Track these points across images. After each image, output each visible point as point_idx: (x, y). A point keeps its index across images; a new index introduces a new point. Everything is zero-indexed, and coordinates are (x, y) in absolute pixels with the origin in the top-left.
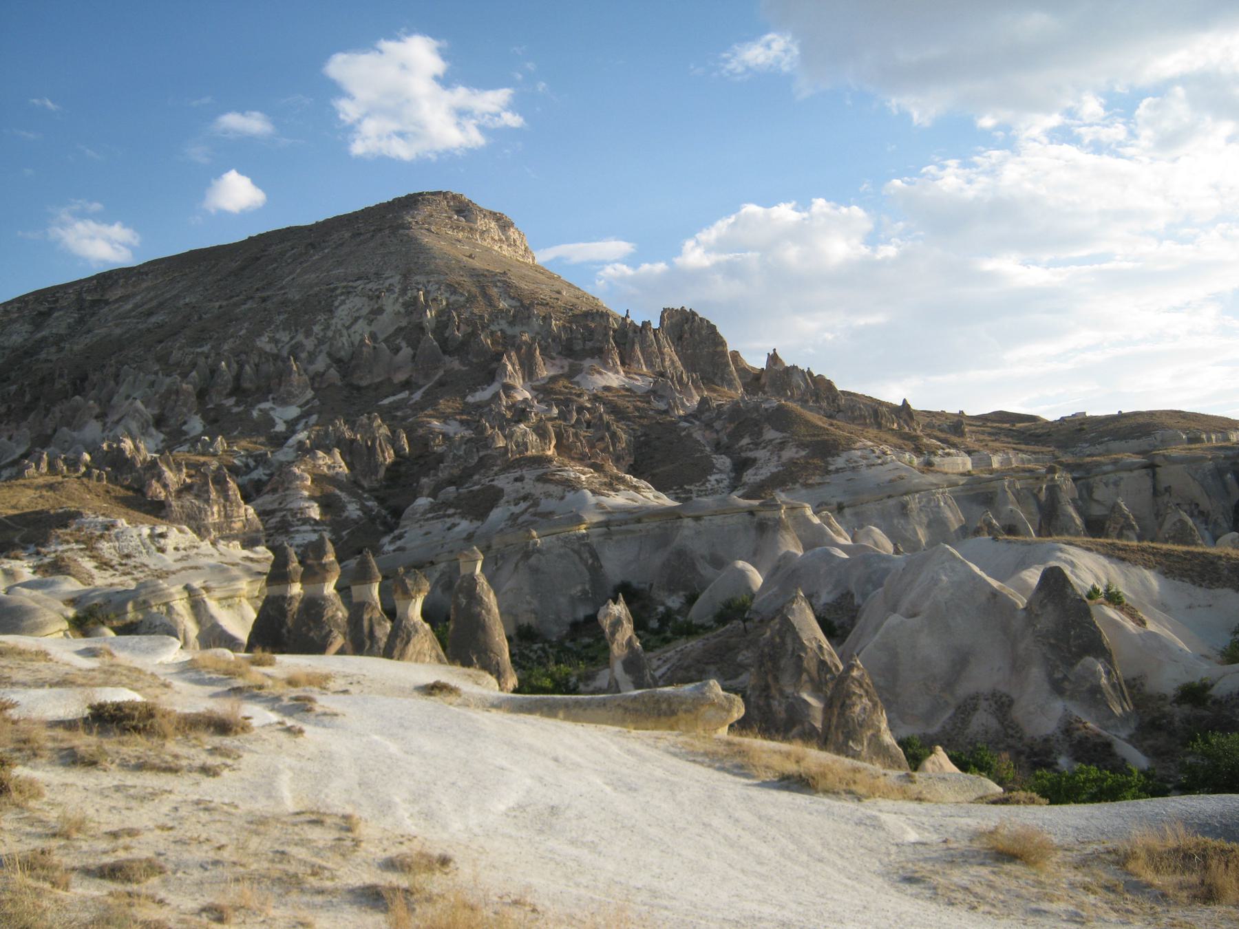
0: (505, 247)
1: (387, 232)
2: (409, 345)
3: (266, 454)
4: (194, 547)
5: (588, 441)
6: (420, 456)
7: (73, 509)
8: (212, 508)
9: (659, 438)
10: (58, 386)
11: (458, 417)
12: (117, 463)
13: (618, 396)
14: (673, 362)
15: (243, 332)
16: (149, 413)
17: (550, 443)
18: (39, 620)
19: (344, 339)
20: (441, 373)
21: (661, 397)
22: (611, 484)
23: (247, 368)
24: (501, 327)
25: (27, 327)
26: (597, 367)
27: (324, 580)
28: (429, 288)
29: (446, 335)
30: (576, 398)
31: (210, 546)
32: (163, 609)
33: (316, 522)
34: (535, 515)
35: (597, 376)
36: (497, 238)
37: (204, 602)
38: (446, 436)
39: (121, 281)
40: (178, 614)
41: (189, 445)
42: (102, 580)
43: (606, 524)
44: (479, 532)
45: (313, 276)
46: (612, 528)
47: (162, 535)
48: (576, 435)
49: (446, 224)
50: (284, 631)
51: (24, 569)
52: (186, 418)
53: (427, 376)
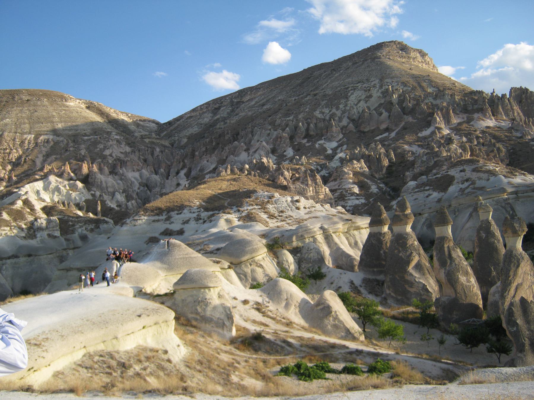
0: (424, 65)
1: (370, 61)
2: (386, 111)
3: (326, 164)
4: (313, 207)
5: (485, 152)
6: (401, 162)
7: (251, 189)
8: (309, 188)
9: (520, 150)
10: (227, 138)
11: (416, 143)
12: (262, 168)
13: (495, 131)
14: (518, 114)
15: (307, 109)
16: (269, 147)
17: (468, 154)
18: (254, 247)
19: (355, 110)
20: (403, 123)
21: (517, 130)
22: (512, 172)
23: (312, 125)
24: (430, 101)
25: (211, 115)
26: (481, 117)
27: (406, 224)
28: (393, 84)
29: (404, 106)
30: (473, 132)
31: (321, 206)
32: (311, 240)
33: (358, 195)
34: (474, 189)
35: (482, 122)
36: (420, 61)
37: (331, 235)
38: (413, 153)
39: (249, 93)
40: (319, 242)
41: (288, 161)
42: (273, 224)
43: (516, 193)
44: (444, 198)
45: (337, 83)
46: (519, 195)
47: (297, 201)
48: (480, 149)
49: (397, 55)
50: (382, 252)
51: (234, 217)
52: (285, 149)
53: (397, 125)
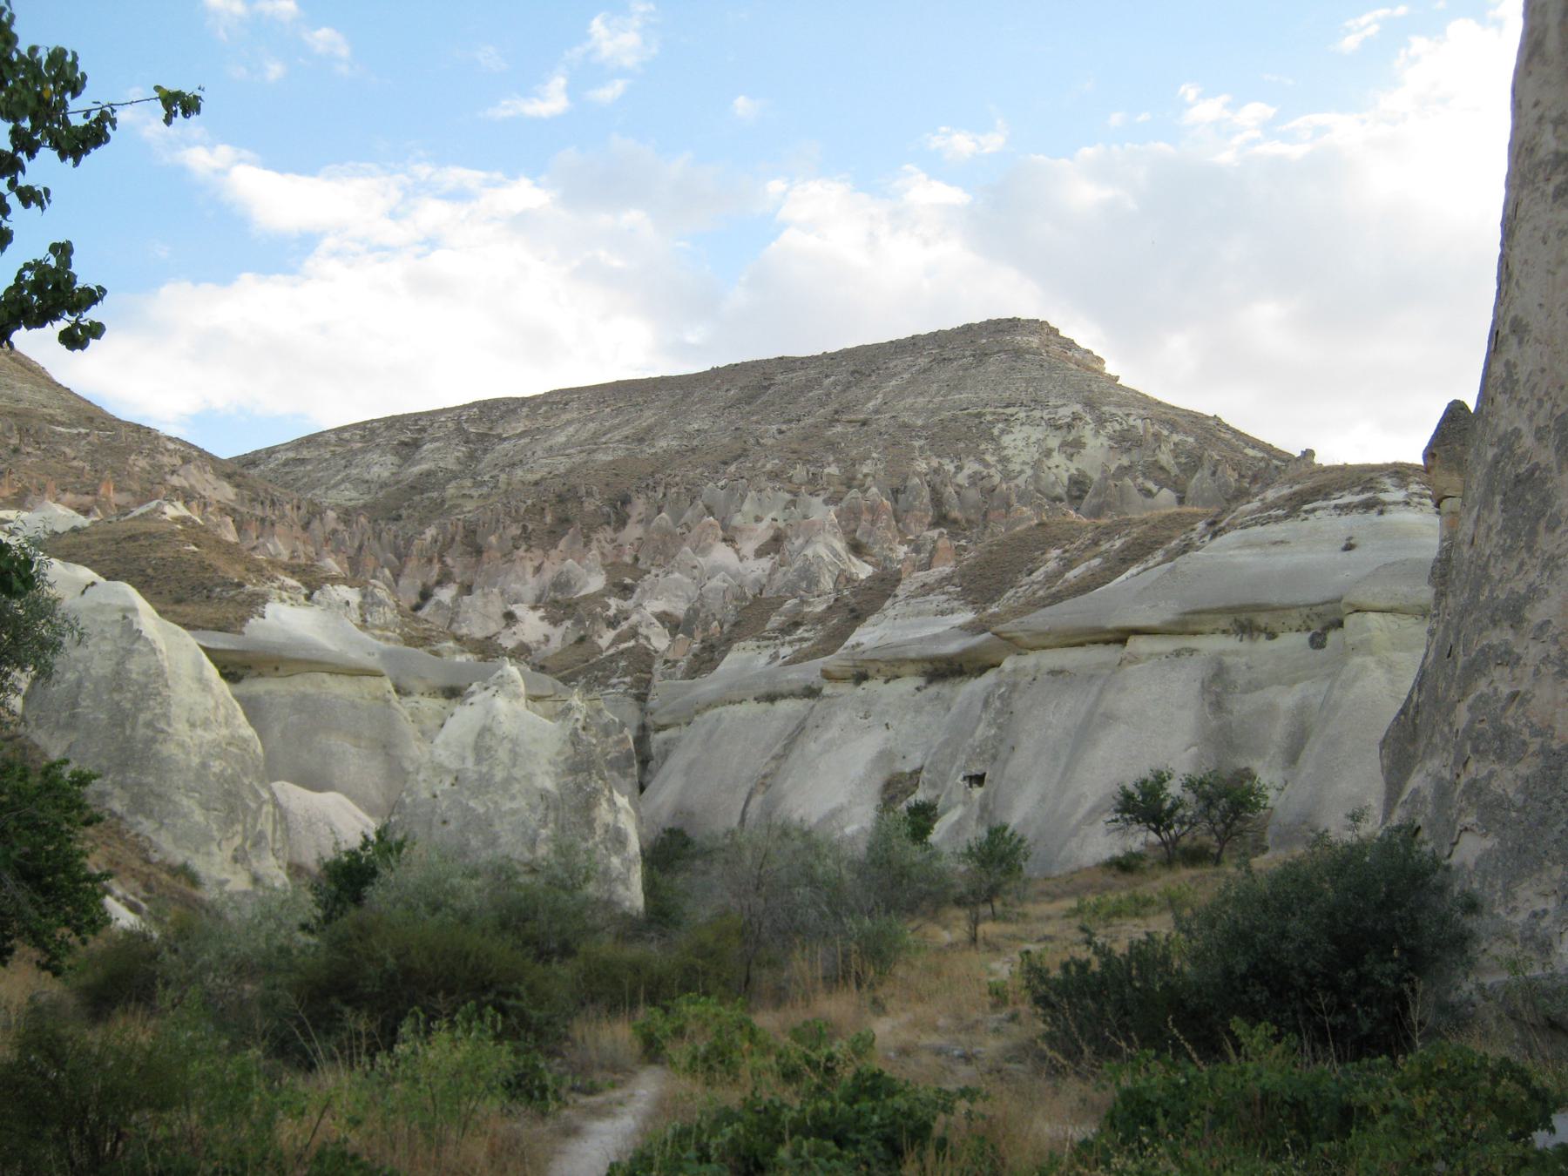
10: (590, 505)
